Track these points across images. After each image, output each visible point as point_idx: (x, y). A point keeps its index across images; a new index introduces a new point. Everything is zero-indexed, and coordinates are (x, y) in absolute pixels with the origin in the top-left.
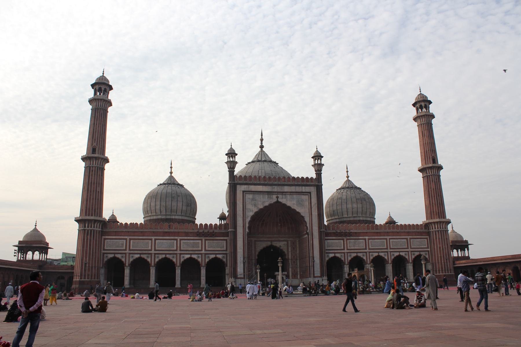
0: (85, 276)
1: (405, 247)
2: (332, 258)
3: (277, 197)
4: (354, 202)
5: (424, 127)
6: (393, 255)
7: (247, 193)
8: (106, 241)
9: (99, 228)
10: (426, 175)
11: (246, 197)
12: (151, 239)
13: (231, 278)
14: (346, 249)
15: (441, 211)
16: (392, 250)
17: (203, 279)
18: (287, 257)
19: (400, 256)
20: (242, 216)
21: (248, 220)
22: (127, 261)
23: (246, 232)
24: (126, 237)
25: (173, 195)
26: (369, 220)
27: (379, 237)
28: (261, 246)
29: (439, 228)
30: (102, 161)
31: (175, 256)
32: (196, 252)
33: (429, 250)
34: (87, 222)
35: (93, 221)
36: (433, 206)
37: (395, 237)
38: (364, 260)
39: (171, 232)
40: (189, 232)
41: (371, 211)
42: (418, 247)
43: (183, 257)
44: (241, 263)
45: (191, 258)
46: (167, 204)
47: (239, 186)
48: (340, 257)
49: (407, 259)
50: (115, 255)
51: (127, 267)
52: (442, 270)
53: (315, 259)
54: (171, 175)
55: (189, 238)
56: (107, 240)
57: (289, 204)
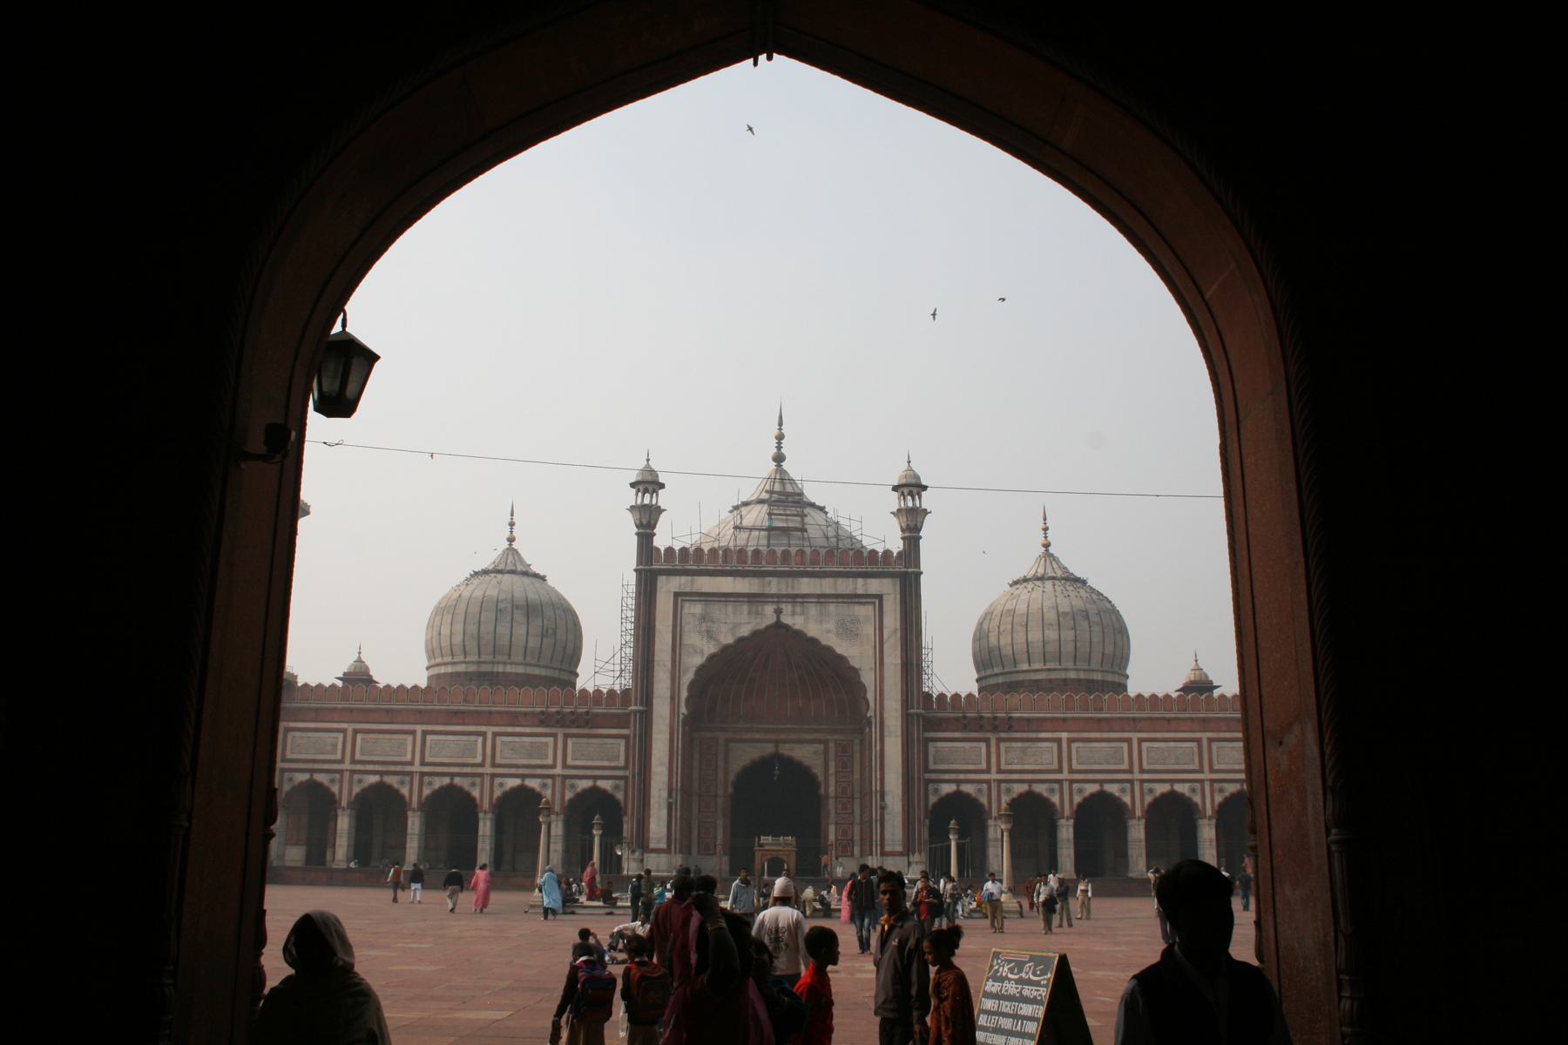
1: (1191, 767)
2: (949, 796)
3: (778, 612)
4: (1050, 624)
6: (1151, 791)
7: (688, 598)
8: (290, 735)
12: (413, 733)
14: (994, 769)
17: (556, 851)
18: (822, 791)
19: (1172, 794)
20: (670, 666)
21: (687, 678)
22: (345, 793)
23: (678, 716)
24: (344, 726)
25: (501, 606)
26: (1098, 681)
27: (1105, 735)
28: (746, 754)
31: (478, 780)
32: (539, 771)
37: (1158, 735)
38: (1053, 805)
39: (470, 713)
40: (520, 713)
41: (1106, 652)
43: (501, 785)
44: (660, 805)
45: (522, 789)
47: (664, 577)
48: (974, 795)
49: (1196, 804)
50: (312, 775)
51: (344, 810)
53: (888, 799)
54: (510, 545)
55: (518, 729)
56: (293, 733)
57: (813, 630)
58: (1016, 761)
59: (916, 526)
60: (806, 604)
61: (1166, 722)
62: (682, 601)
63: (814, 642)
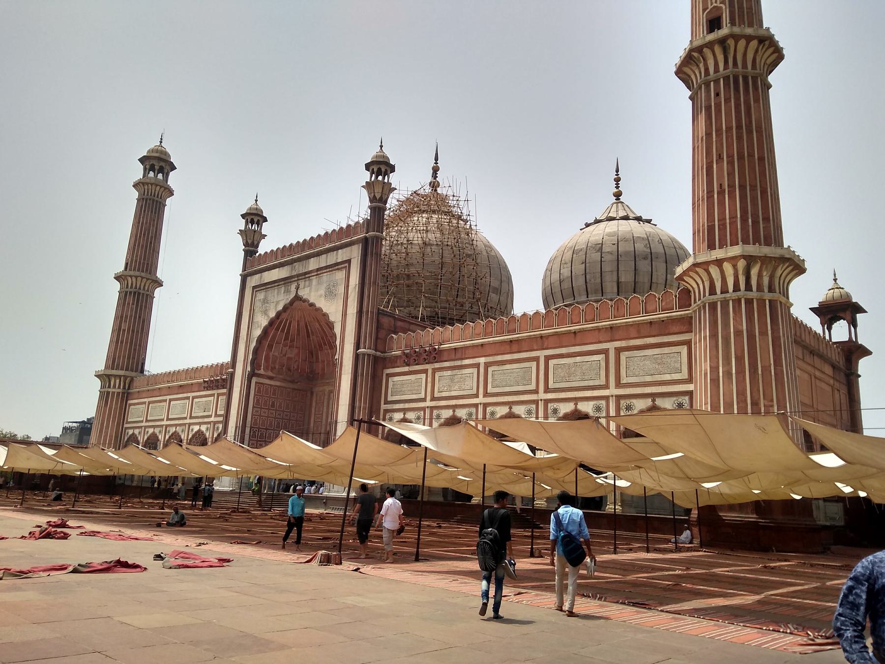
1: (597, 383)
3: (297, 288)
7: (258, 289)
8: (132, 407)
9: (119, 387)
11: (257, 298)
14: (428, 398)
15: (722, 220)
16: (550, 396)
21: (253, 345)
29: (707, 294)
30: (134, 279)
32: (206, 420)
37: (563, 351)
41: (622, 279)
42: (648, 379)
58: (445, 389)
59: (374, 195)
60: (311, 278)
61: (573, 335)
62: (256, 291)
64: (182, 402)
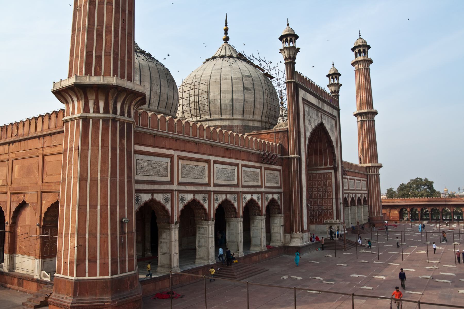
0: (123, 262)
5: (366, 71)
10: (367, 119)
13: (300, 233)
21: (307, 142)
24: (172, 152)
32: (258, 190)
33: (367, 192)
34: (122, 101)
35: (140, 98)
36: (373, 150)
46: (161, 92)
50: (153, 195)
52: (379, 212)
63: (327, 133)
64: (229, 167)
